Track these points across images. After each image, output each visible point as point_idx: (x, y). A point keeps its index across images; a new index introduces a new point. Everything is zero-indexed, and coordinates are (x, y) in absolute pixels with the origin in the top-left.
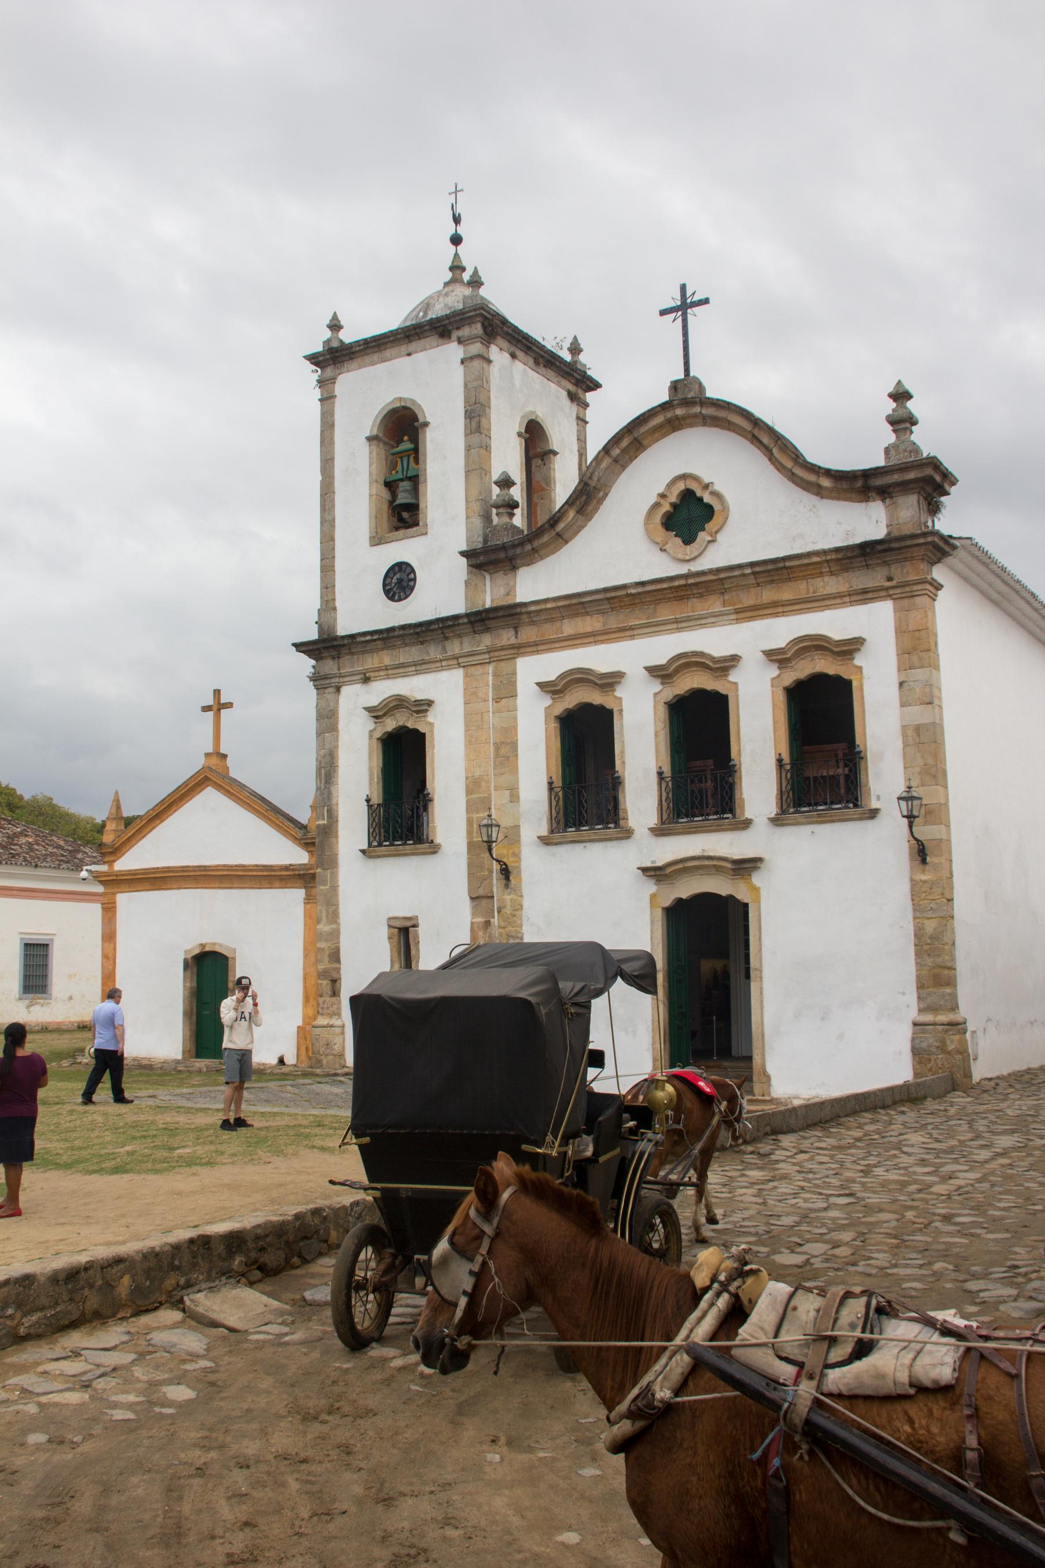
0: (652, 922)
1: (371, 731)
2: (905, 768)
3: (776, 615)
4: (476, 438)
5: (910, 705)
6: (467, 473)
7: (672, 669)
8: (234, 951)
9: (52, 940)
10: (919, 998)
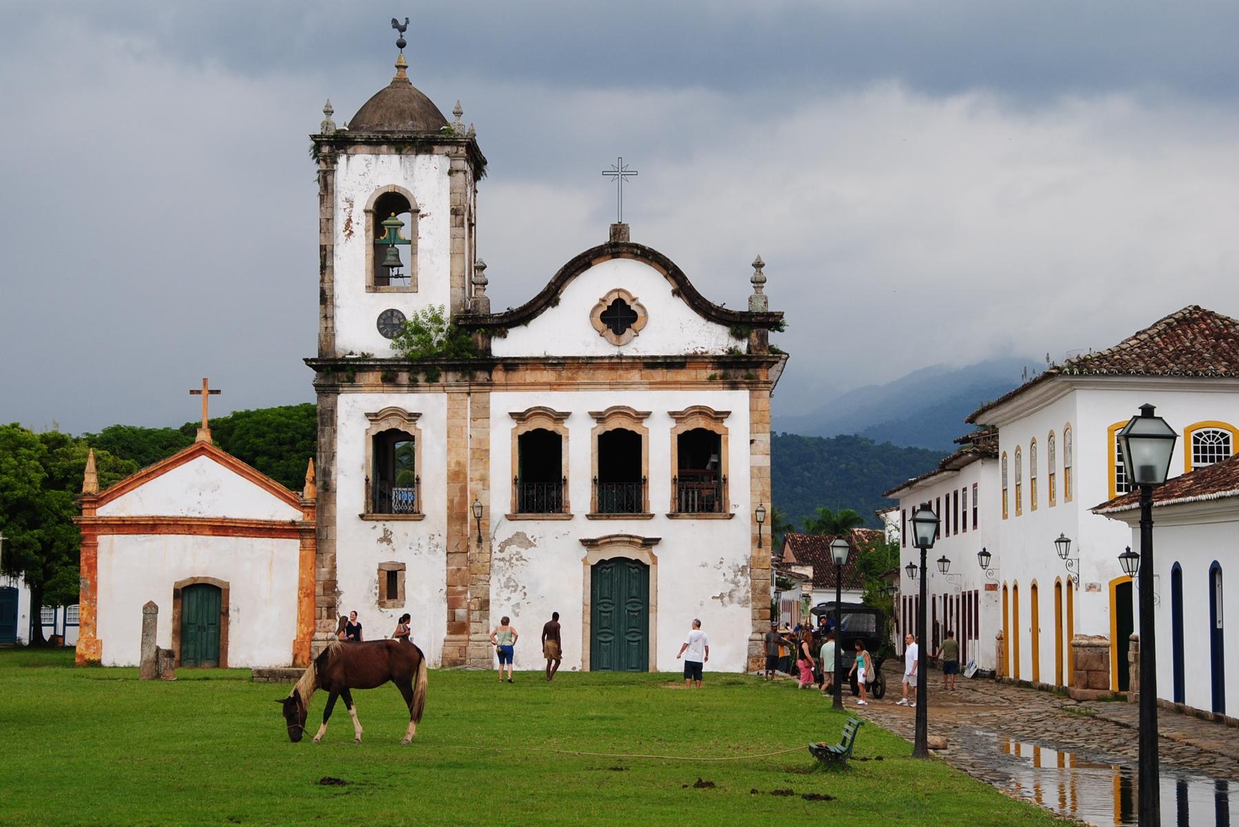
0: (584, 574)
1: (367, 430)
3: (676, 389)
4: (459, 231)
5: (756, 454)
6: (452, 255)
7: (607, 415)
8: (229, 583)
10: (753, 625)
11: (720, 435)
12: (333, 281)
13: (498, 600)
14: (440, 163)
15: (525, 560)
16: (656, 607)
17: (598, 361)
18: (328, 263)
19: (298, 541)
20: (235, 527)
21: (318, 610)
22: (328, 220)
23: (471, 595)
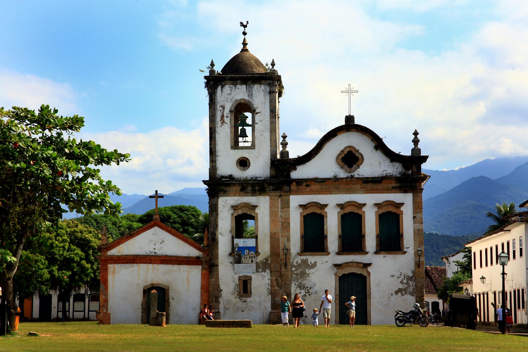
0: (336, 281)
1: (232, 214)
2: (414, 241)
5: (416, 223)
7: (345, 205)
8: (168, 286)
12: (215, 144)
14: (265, 88)
15: (308, 275)
16: (370, 296)
17: (341, 180)
18: (213, 136)
19: (201, 266)
20: (171, 260)
21: (211, 299)
22: (213, 116)
23: (282, 291)
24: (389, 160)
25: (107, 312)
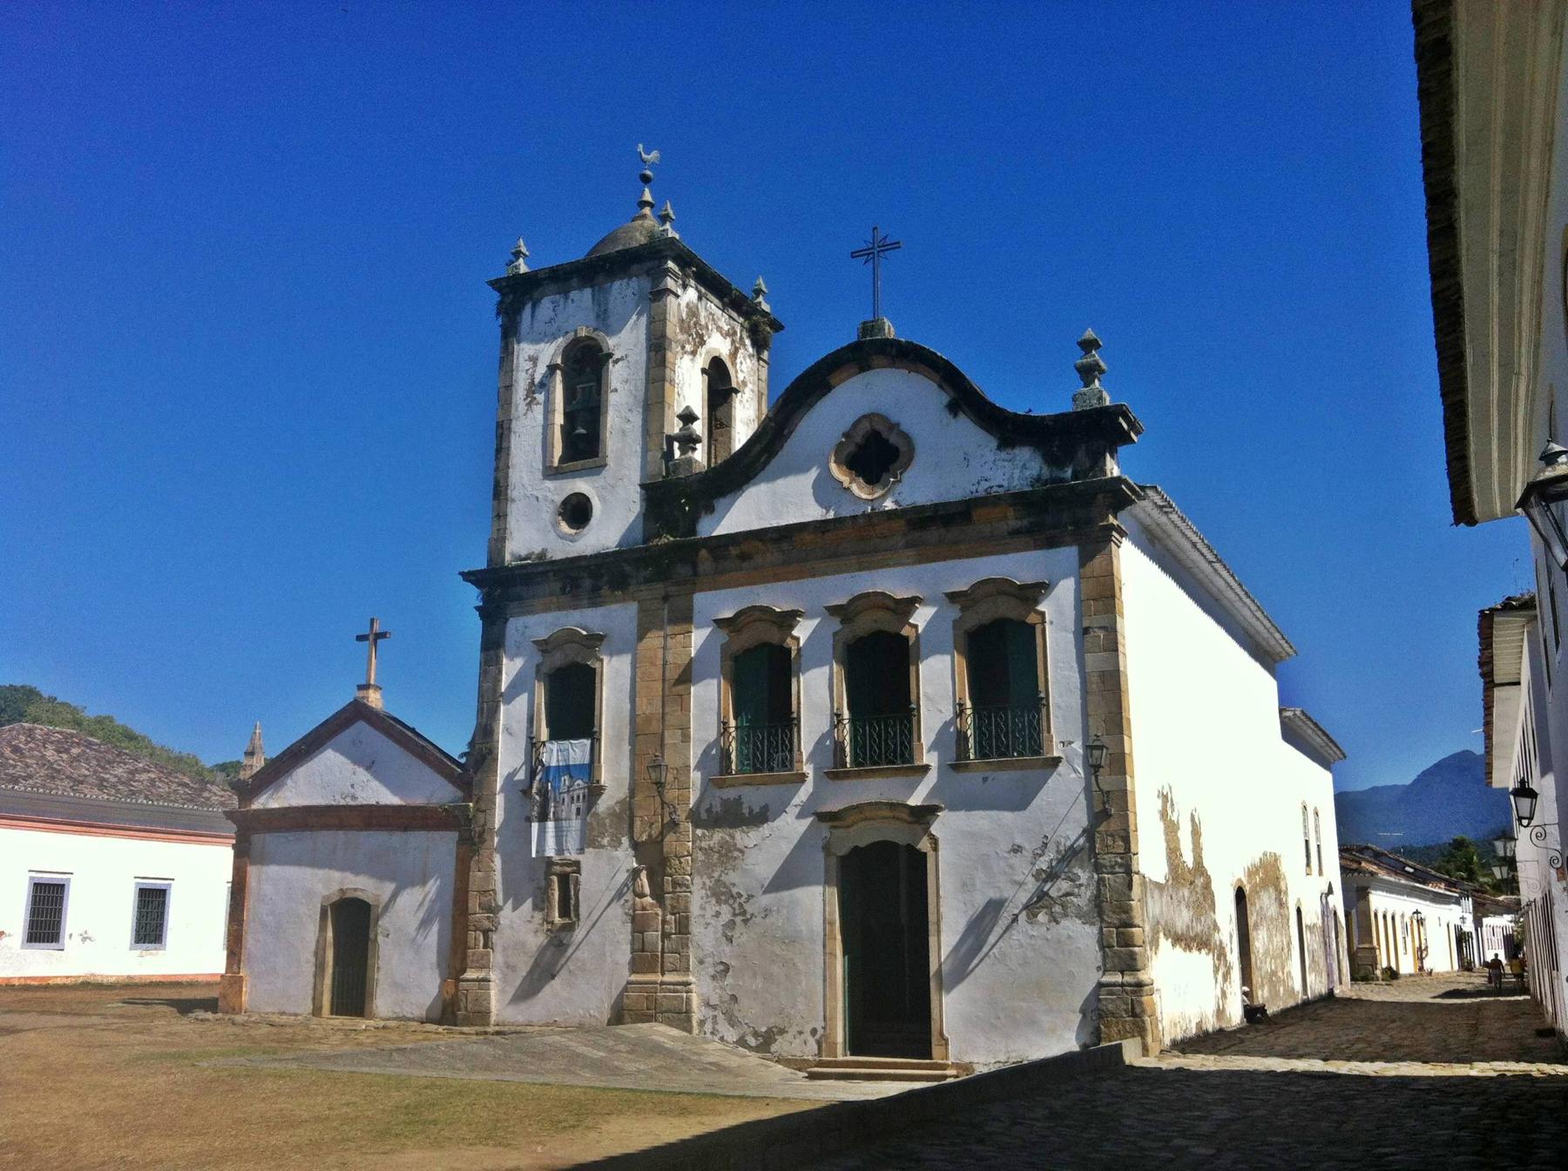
1: (538, 666)
9: (170, 885)
11: (1033, 627)
12: (508, 467)
13: (703, 916)
15: (741, 851)
18: (505, 445)
24: (994, 443)
25: (239, 973)
